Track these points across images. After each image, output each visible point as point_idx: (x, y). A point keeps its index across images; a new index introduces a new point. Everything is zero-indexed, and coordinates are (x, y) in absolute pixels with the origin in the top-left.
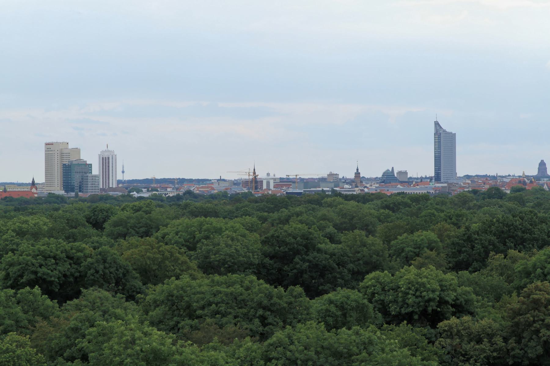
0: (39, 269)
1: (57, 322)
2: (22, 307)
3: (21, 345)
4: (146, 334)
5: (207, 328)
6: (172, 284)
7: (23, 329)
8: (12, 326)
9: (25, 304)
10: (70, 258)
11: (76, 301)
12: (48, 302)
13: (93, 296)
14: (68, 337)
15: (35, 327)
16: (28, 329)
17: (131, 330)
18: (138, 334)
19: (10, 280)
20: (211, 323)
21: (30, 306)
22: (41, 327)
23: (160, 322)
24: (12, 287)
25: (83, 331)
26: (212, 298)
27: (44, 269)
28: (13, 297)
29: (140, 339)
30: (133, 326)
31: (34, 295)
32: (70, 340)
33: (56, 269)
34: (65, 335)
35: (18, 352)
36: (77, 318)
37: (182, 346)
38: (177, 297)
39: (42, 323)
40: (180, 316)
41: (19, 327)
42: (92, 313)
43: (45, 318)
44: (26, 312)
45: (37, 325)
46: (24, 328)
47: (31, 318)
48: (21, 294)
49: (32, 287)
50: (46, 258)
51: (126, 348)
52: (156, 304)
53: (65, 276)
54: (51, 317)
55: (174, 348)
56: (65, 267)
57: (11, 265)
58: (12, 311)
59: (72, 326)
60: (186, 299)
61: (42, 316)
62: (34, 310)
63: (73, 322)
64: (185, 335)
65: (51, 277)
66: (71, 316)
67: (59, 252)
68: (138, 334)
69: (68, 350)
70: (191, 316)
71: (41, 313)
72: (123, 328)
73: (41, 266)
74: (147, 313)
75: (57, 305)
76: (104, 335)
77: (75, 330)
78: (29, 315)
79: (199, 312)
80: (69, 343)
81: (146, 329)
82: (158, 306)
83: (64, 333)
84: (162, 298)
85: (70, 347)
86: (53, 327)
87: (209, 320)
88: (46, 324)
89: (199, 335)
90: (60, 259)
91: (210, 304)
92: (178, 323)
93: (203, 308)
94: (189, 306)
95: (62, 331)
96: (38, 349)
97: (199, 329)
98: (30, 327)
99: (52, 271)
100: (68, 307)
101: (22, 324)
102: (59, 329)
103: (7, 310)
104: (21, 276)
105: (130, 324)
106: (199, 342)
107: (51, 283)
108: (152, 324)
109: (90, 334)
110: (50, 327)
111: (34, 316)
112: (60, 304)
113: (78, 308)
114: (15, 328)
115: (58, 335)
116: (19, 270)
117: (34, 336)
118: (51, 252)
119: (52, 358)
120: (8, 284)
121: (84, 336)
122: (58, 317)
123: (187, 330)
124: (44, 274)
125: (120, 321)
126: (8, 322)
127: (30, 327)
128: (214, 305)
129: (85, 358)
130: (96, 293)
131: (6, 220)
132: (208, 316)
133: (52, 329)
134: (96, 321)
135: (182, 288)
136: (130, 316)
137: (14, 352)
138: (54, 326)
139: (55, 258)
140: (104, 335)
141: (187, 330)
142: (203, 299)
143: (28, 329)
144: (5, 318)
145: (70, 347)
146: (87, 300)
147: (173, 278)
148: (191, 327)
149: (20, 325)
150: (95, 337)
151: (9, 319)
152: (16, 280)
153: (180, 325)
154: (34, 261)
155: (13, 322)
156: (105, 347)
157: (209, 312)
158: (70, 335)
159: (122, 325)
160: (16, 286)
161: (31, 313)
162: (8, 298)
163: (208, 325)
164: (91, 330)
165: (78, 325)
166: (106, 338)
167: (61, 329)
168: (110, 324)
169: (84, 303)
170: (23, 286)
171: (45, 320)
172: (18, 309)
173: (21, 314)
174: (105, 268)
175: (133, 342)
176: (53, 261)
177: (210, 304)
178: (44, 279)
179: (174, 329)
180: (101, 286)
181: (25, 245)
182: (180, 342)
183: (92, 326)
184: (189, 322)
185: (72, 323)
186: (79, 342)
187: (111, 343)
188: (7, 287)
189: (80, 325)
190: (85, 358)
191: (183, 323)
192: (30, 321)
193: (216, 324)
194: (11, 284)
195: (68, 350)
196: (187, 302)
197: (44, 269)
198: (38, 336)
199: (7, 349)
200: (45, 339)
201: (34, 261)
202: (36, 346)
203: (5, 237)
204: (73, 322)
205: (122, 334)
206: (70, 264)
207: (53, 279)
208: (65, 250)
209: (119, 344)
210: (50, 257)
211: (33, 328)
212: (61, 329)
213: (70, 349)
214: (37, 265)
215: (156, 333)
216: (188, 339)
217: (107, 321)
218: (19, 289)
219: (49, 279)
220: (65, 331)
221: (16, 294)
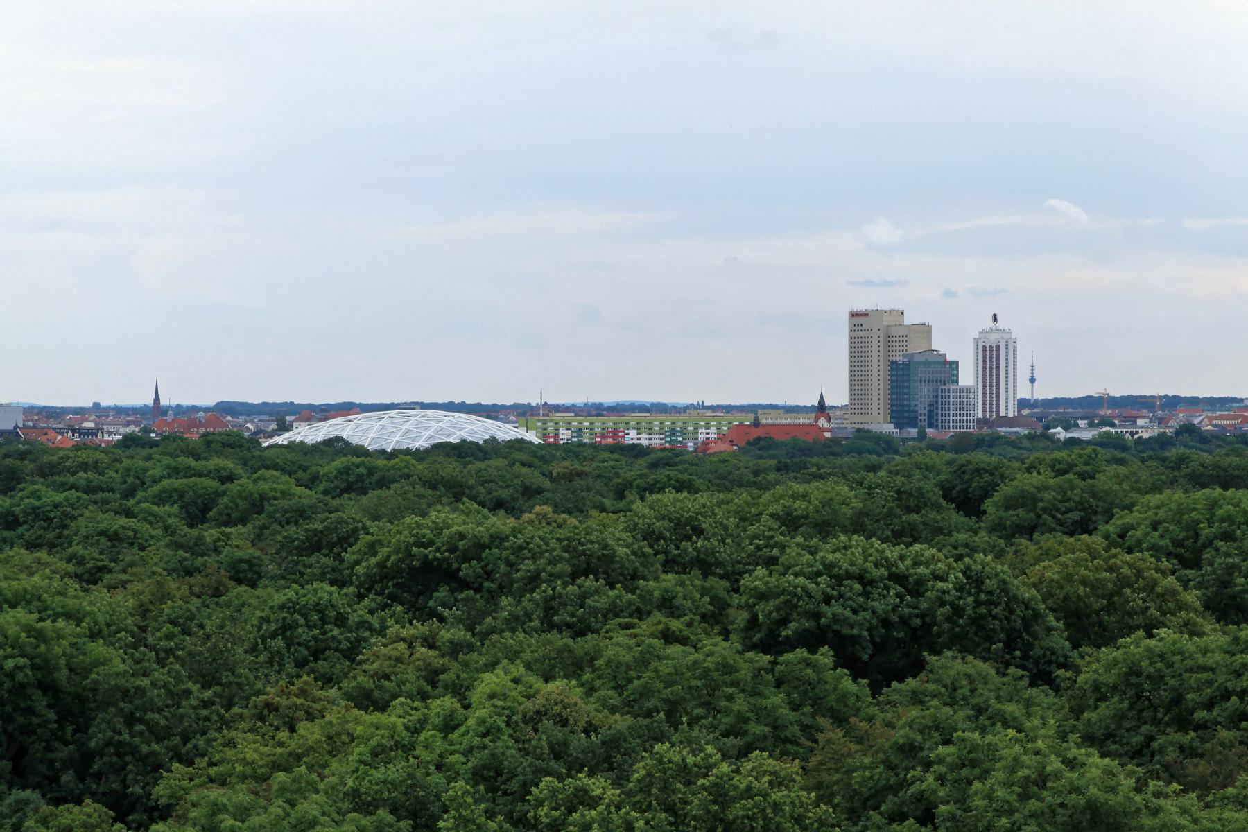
0: (824, 607)
1: (866, 731)
2: (788, 694)
3: (779, 782)
4: (1071, 764)
5: (1220, 753)
6: (1135, 646)
7: (789, 746)
8: (765, 738)
9: (796, 687)
10: (900, 579)
11: (912, 683)
12: (848, 684)
13: (952, 672)
14: (891, 767)
15: (816, 741)
16: (798, 744)
17: (1037, 753)
18: (1055, 764)
19: (759, 632)
20: (1230, 741)
21: (805, 692)
22: (829, 741)
23: (1109, 736)
24: (764, 648)
25: (925, 753)
26: (1230, 680)
27: (836, 608)
28: (767, 671)
29: (1057, 775)
30: (1039, 744)
31: (815, 667)
32: (897, 775)
33: (864, 610)
34: (883, 762)
35: (776, 795)
36: (912, 721)
37: (1157, 795)
38: (1149, 676)
39: (831, 734)
40: (1155, 721)
41: (780, 743)
42: (947, 710)
43: (839, 720)
44: (795, 707)
45: (821, 737)
46: (792, 742)
47: (807, 721)
48: (787, 663)
49: (813, 651)
50: (839, 580)
51: (1024, 797)
52: (1099, 692)
53: (886, 623)
54: (852, 720)
55: (1138, 798)
56: (885, 602)
57: (762, 596)
58: (765, 702)
59: (901, 741)
60: (1172, 682)
61: (832, 717)
62: (817, 703)
63: (902, 732)
64: (1166, 767)
65: (852, 627)
66: (899, 718)
67: (869, 565)
68: (1055, 764)
69: (891, 797)
70: (1183, 724)
71: (831, 709)
72: (1017, 748)
73: (828, 600)
74: (1077, 712)
75: (868, 691)
76: (974, 764)
77: (909, 750)
78: (803, 714)
79: (1201, 714)
80: (892, 781)
81: (1074, 752)
82: (1104, 698)
83: (881, 756)
84: (1110, 678)
85: (894, 789)
86: (858, 743)
87: (1223, 734)
88: (841, 734)
89: (1198, 768)
90: (871, 582)
91: (1226, 695)
92: (1151, 738)
93: (1209, 706)
94: (1177, 700)
95: (877, 752)
96: (821, 793)
97: (1201, 756)
98: (803, 740)
99: (855, 612)
100: (895, 697)
101: (788, 733)
102: (871, 747)
103: (752, 701)
104: (784, 622)
105: (1033, 740)
106: (1201, 786)
107: (855, 640)
108: (1089, 739)
109: (941, 761)
110: (851, 742)
111: (813, 715)
112: (875, 690)
113: (917, 699)
114: (770, 741)
115: (867, 761)
116: (778, 609)
117: (814, 761)
118: (852, 564)
119: (854, 815)
120: (754, 640)
121: (927, 765)
122: (870, 719)
123: (1171, 755)
124: (836, 619)
125: (1011, 733)
126: (757, 729)
127: (803, 740)
128: (1234, 699)
129: (927, 817)
130: (958, 665)
131: (755, 492)
132: (1220, 723)
133: (854, 747)
134: (956, 730)
135: (1161, 656)
136: (1036, 722)
137: (765, 795)
138: (860, 741)
139: (861, 578)
140: (974, 764)
141: (1171, 755)
142: (1210, 683)
143: (798, 744)
144: (749, 719)
145: (894, 789)
146: (938, 681)
147: (1141, 633)
148: (1182, 749)
149: (783, 736)
150: (952, 768)
151: (758, 721)
152: (773, 634)
153: (1155, 745)
154: (812, 586)
155: (767, 729)
156: (976, 794)
157: (1224, 714)
158: (895, 760)
159: (1017, 741)
160: (772, 644)
161: (807, 709)
162: (757, 674)
163: (1223, 744)
164: (942, 750)
165: (914, 739)
166: (977, 771)
167: (875, 748)
168: (989, 738)
169: (931, 687)
170: (790, 645)
171: (838, 727)
172: (776, 699)
173: (785, 711)
174: (978, 603)
175: (1042, 780)
176: (858, 587)
177: (1226, 695)
178: (837, 633)
179: (1138, 754)
180: (966, 649)
181: (795, 549)
182: (1153, 785)
183: (947, 742)
184: (1177, 737)
185: (901, 735)
186: (915, 780)
187: (989, 783)
188: (753, 647)
189: (919, 738)
190: (927, 817)
191: (1161, 740)
192: (805, 728)
193: (1241, 743)
194: (761, 640)
195: (891, 797)
196: (1173, 689)
197: (836, 608)
198: (821, 763)
199: (749, 788)
200: (837, 770)
201: (812, 586)
202: (818, 786)
203: (752, 530)
204: (902, 732)
205: (1016, 763)
206: (898, 595)
207: (855, 632)
208: (887, 560)
209: (1008, 784)
210: (849, 576)
211: (809, 744)
212: (875, 748)
213: (896, 795)
214: (820, 597)
215: (1096, 763)
216: (1173, 778)
217: (983, 731)
218: (781, 653)
219: (846, 631)
220: (885, 753)
221: (774, 663)
